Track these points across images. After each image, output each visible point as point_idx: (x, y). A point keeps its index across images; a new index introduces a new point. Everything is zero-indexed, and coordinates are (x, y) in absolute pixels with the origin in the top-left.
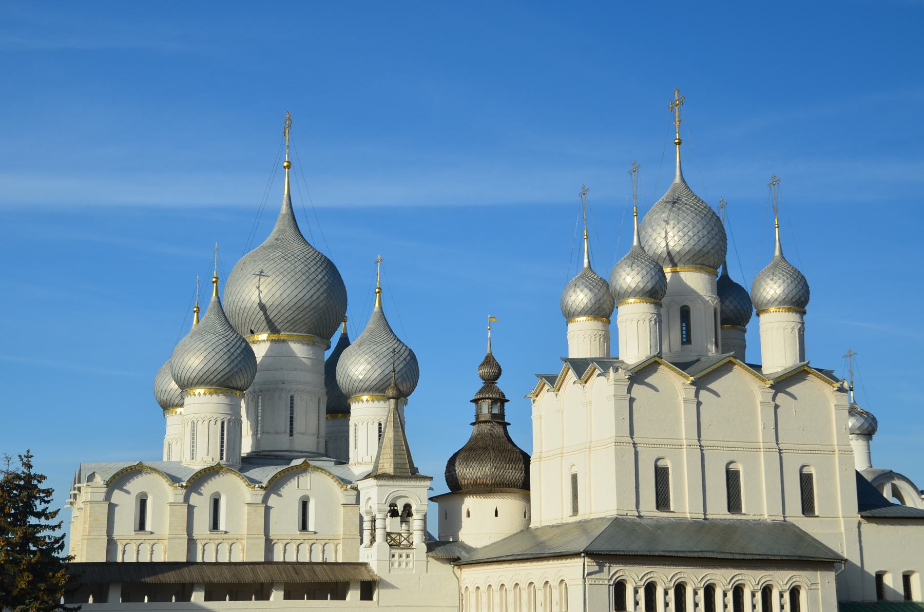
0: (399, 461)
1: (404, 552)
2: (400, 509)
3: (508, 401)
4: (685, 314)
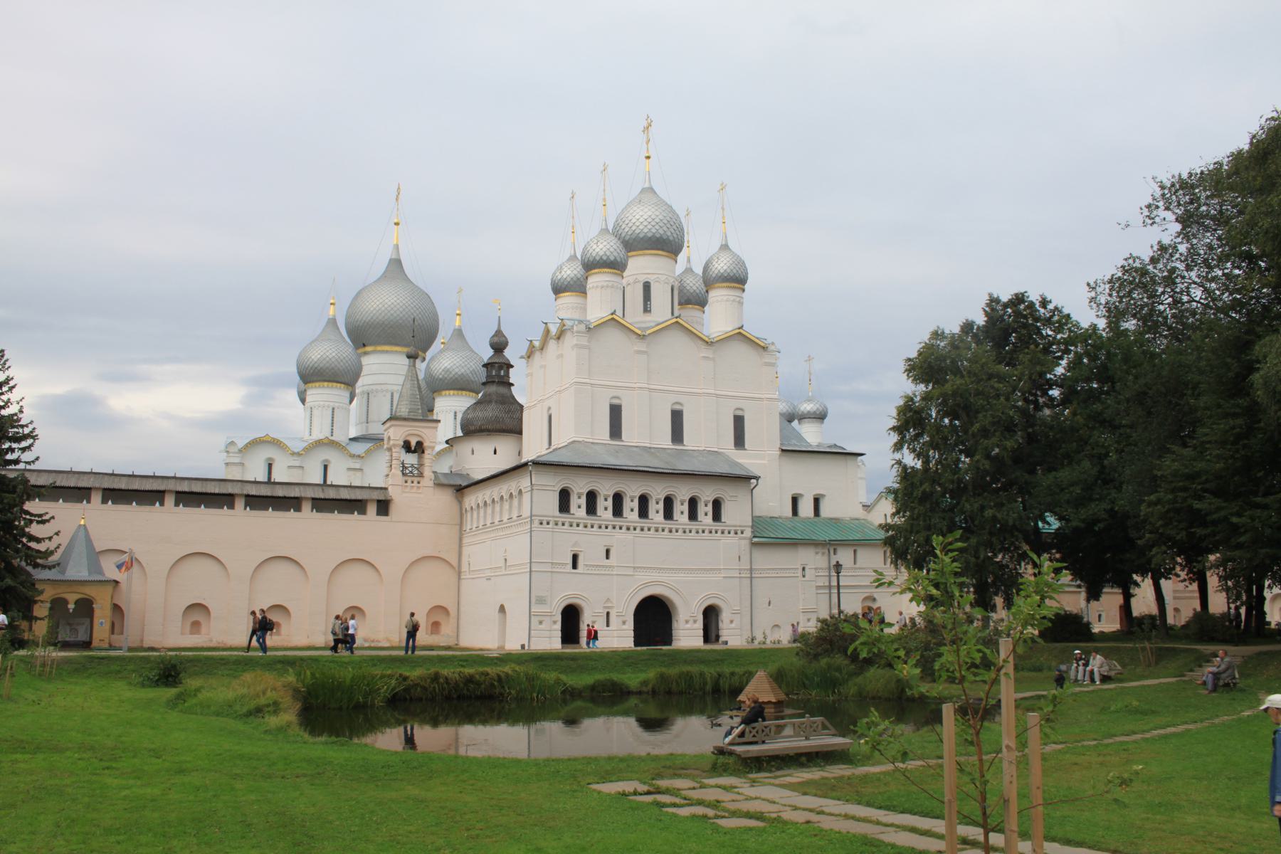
0: (413, 407)
1: (416, 480)
2: (413, 444)
3: (512, 366)
4: (647, 287)
